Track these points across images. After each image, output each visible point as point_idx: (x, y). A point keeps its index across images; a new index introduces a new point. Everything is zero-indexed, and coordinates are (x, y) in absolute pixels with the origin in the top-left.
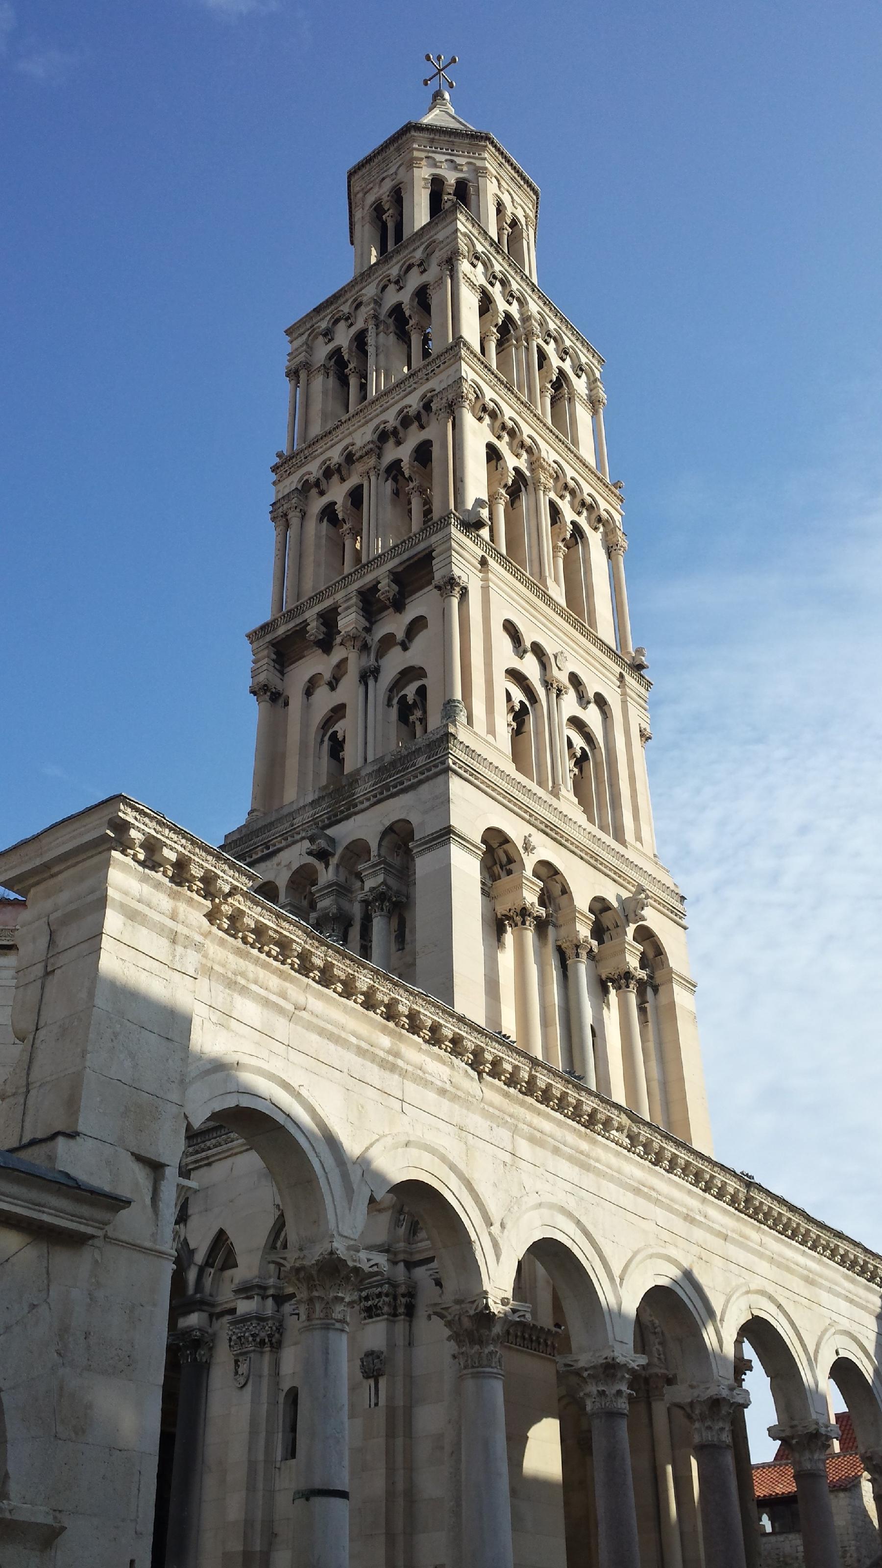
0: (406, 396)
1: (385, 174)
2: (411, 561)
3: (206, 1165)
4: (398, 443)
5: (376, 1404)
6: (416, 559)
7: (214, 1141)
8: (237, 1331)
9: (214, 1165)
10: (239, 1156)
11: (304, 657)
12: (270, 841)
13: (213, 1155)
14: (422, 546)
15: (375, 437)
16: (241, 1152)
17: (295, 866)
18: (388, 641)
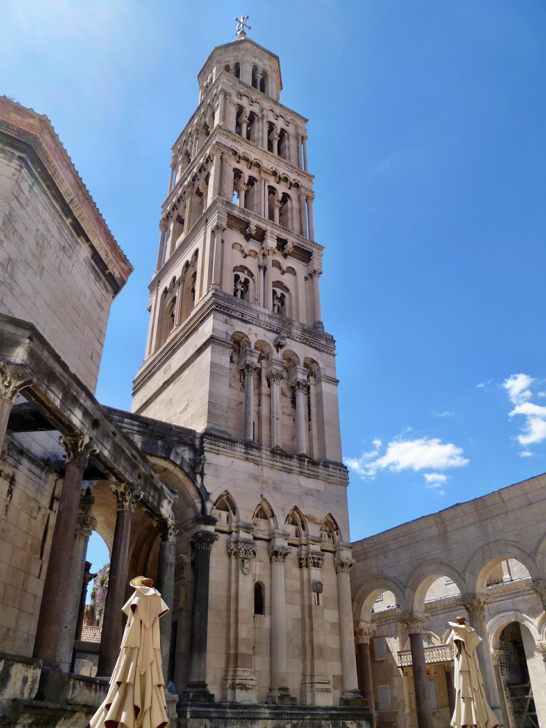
0: (290, 172)
1: (262, 60)
2: (301, 247)
3: (215, 453)
4: (278, 183)
5: (318, 604)
6: (303, 248)
7: (224, 445)
8: (245, 546)
9: (220, 456)
10: (236, 459)
11: (232, 229)
12: (246, 315)
13: (223, 451)
14: (309, 247)
15: (272, 170)
16: (239, 459)
17: (261, 338)
18: (276, 264)
